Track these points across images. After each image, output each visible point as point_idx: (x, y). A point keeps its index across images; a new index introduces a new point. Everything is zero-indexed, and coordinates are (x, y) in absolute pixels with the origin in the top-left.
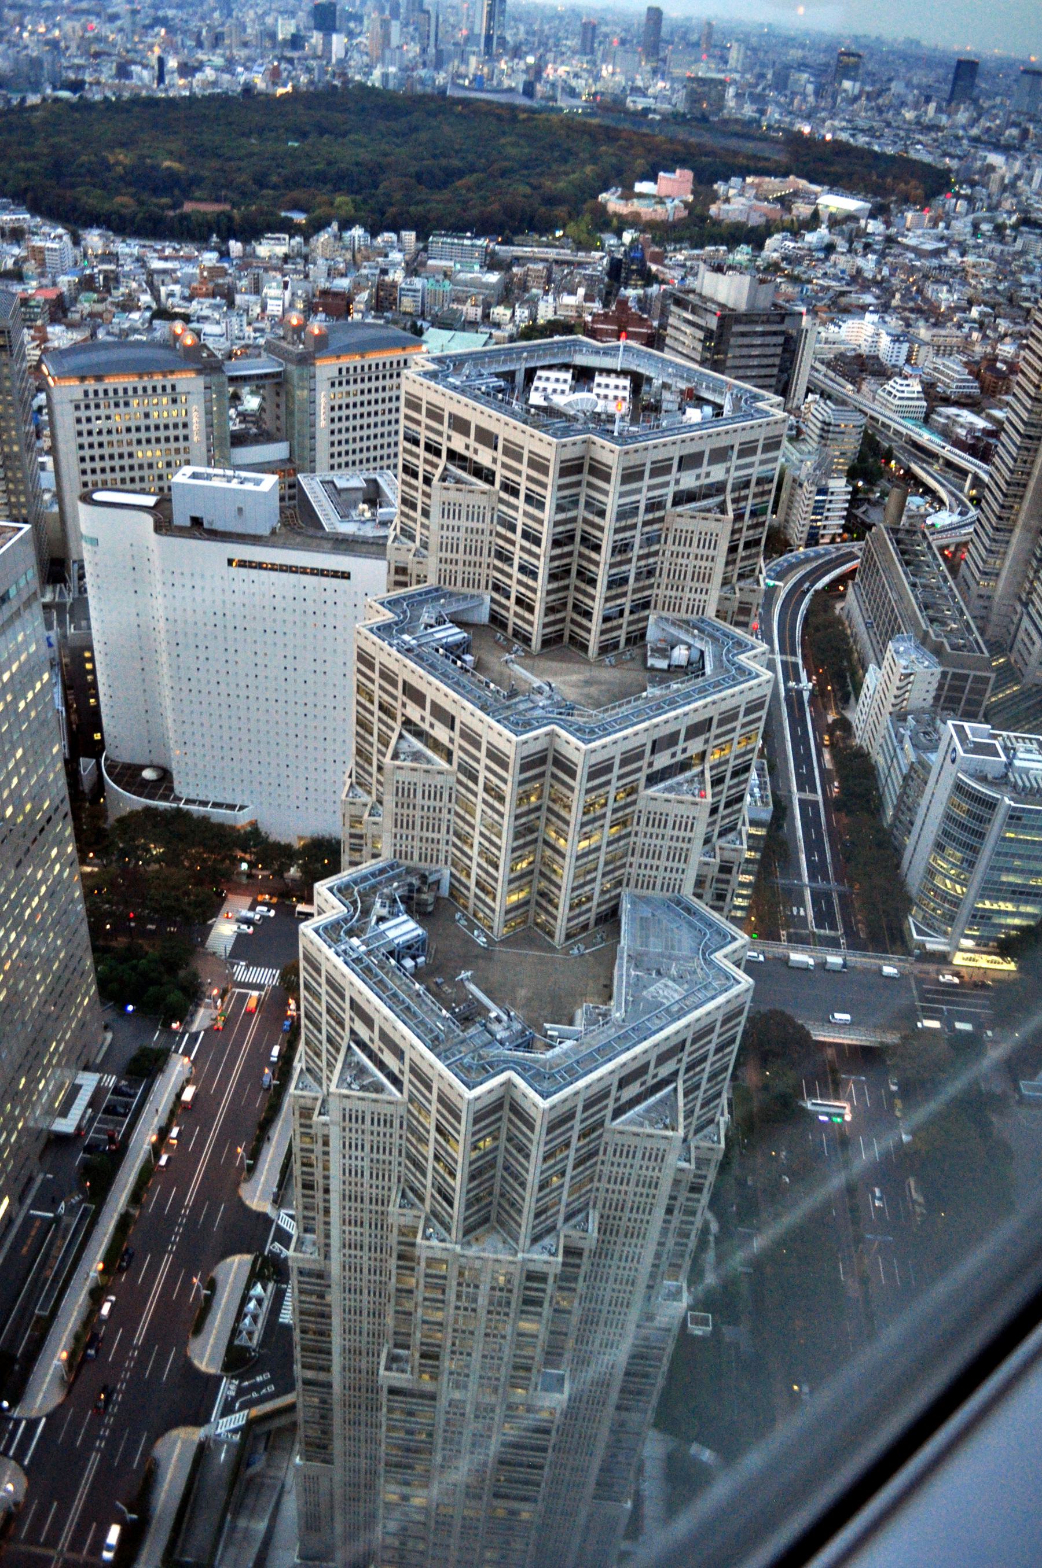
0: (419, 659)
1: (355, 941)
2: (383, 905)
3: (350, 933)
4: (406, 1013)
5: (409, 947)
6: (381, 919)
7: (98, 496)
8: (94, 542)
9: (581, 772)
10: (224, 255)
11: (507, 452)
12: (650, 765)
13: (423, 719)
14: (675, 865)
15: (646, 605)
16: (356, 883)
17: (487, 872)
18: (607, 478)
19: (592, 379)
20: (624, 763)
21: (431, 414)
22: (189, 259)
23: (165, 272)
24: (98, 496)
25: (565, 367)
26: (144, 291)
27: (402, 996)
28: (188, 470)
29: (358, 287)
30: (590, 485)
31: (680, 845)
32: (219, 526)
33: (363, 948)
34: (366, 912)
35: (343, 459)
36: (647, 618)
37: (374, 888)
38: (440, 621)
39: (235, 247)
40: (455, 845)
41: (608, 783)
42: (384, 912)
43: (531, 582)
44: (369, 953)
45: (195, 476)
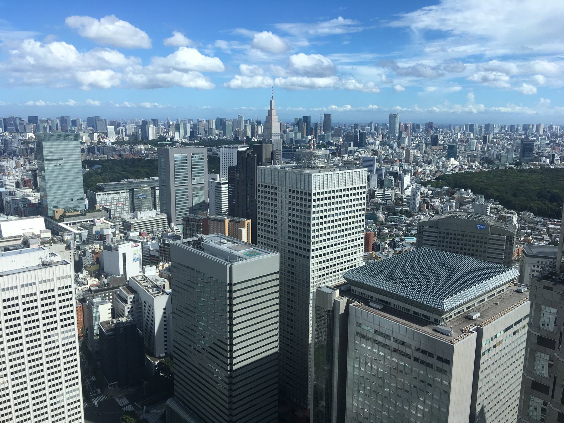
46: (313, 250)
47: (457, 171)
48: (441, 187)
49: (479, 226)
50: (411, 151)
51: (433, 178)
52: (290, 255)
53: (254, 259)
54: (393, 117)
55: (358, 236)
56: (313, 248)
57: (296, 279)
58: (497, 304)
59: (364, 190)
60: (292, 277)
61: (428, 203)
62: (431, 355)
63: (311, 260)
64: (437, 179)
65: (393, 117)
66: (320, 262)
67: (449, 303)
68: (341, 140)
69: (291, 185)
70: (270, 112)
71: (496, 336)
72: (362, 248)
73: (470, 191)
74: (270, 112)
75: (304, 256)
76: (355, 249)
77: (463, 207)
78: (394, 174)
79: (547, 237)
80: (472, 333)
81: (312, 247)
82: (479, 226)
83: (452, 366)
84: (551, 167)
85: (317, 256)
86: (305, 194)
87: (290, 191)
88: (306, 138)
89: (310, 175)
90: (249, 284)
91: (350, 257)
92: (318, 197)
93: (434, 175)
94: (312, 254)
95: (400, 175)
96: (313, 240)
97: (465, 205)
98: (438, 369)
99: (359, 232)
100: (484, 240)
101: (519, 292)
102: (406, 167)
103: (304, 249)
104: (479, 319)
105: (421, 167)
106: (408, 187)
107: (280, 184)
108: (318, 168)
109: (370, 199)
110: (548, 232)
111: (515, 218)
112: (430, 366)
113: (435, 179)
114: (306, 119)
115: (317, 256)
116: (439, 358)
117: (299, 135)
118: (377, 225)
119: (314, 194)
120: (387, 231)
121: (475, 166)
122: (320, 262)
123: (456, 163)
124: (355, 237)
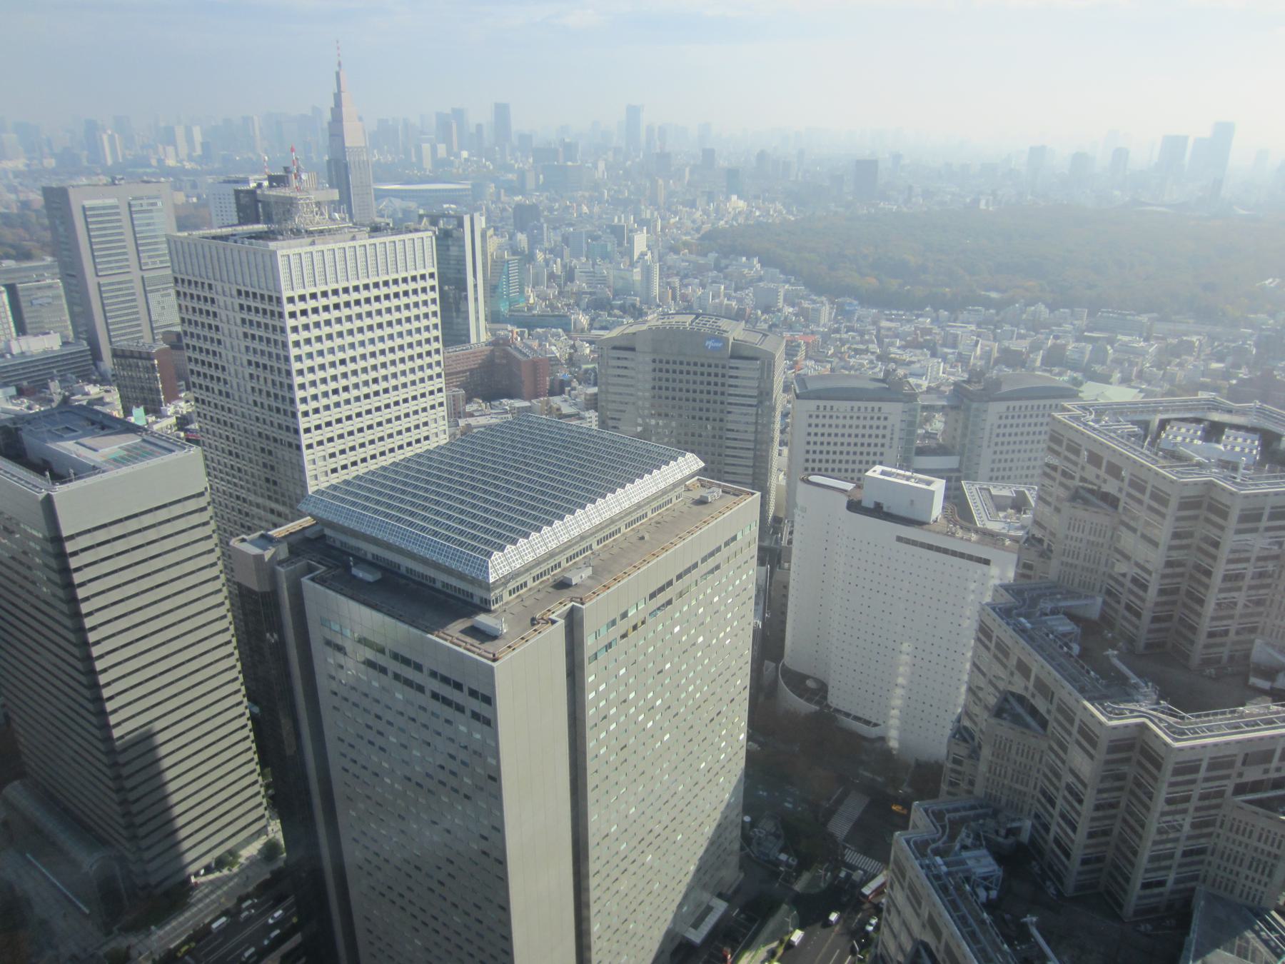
0: (1031, 639)
1: (938, 859)
2: (968, 836)
3: (937, 852)
4: (972, 937)
5: (985, 879)
6: (964, 847)
7: (813, 478)
8: (804, 510)
9: (1168, 767)
10: (936, 320)
11: (1133, 484)
12: (1240, 775)
13: (1026, 688)
14: (1258, 876)
15: (1253, 630)
16: (948, 811)
17: (1066, 834)
18: (1224, 514)
19: (1222, 432)
20: (1212, 767)
21: (1069, 448)
22: (909, 321)
23: (889, 329)
24: (813, 478)
25: (1198, 421)
26: (872, 342)
27: (971, 921)
28: (879, 468)
29: (1035, 348)
30: (1208, 520)
31: (1264, 858)
32: (894, 511)
33: (944, 869)
34: (952, 838)
35: (1001, 474)
36: (1252, 642)
37: (963, 821)
38: (1054, 612)
39: (944, 313)
40: (1039, 801)
41: (1193, 782)
42: (969, 842)
43: (1141, 593)
44: (949, 874)
45: (883, 473)
46: (307, 430)
47: (741, 220)
48: (706, 255)
49: (710, 344)
50: (661, 182)
51: (697, 236)
52: (265, 444)
53: (125, 470)
54: (633, 113)
55: (429, 386)
56: (306, 426)
57: (283, 495)
58: (642, 538)
59: (430, 282)
60: (275, 492)
61: (674, 289)
62: (458, 686)
63: (305, 452)
64: (703, 238)
65: (633, 113)
66: (333, 455)
67: (501, 564)
68: (531, 160)
69: (240, 280)
70: (338, 98)
71: (624, 615)
72: (442, 411)
73: (755, 260)
74: (338, 98)
75: (290, 445)
76: (422, 417)
77: (739, 294)
78: (617, 232)
79: (874, 347)
80: (553, 622)
81: (303, 423)
82: (710, 344)
83: (495, 710)
84: (905, 210)
85: (320, 443)
86: (270, 298)
87: (239, 292)
88: (458, 156)
89: (273, 254)
90: (101, 536)
91: (414, 435)
92: (301, 306)
93: (698, 230)
94: (305, 439)
95: (631, 231)
96: (302, 408)
97: (742, 289)
98: (476, 716)
99: (431, 378)
100: (720, 371)
101: (702, 502)
102: (647, 214)
103: (288, 428)
104: (590, 582)
105: (676, 213)
106: (643, 254)
107: (218, 276)
108: (310, 233)
109: (565, 284)
110: (877, 337)
111: (826, 313)
112: (460, 709)
113: (699, 239)
114: (458, 114)
115: (320, 443)
116: (473, 693)
117: (442, 150)
118: (571, 338)
119: (291, 300)
120: (588, 351)
121: (775, 211)
122: (333, 455)
123: (742, 204)
124: (420, 388)
